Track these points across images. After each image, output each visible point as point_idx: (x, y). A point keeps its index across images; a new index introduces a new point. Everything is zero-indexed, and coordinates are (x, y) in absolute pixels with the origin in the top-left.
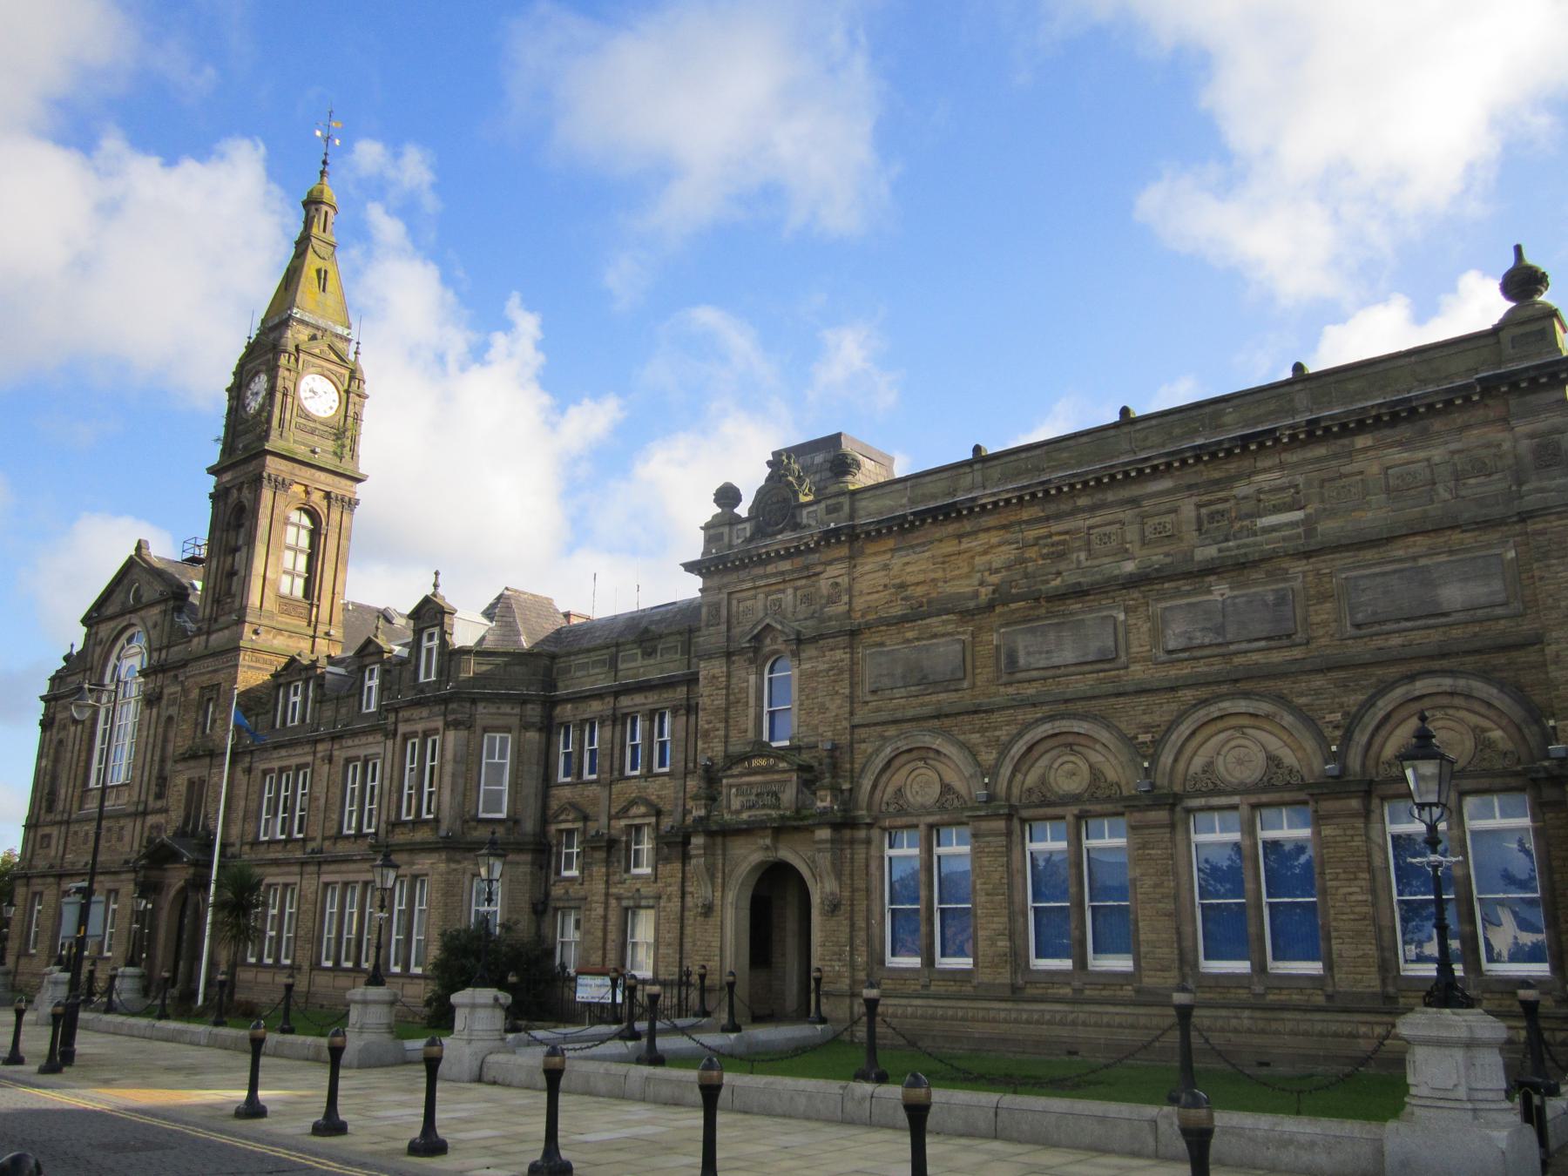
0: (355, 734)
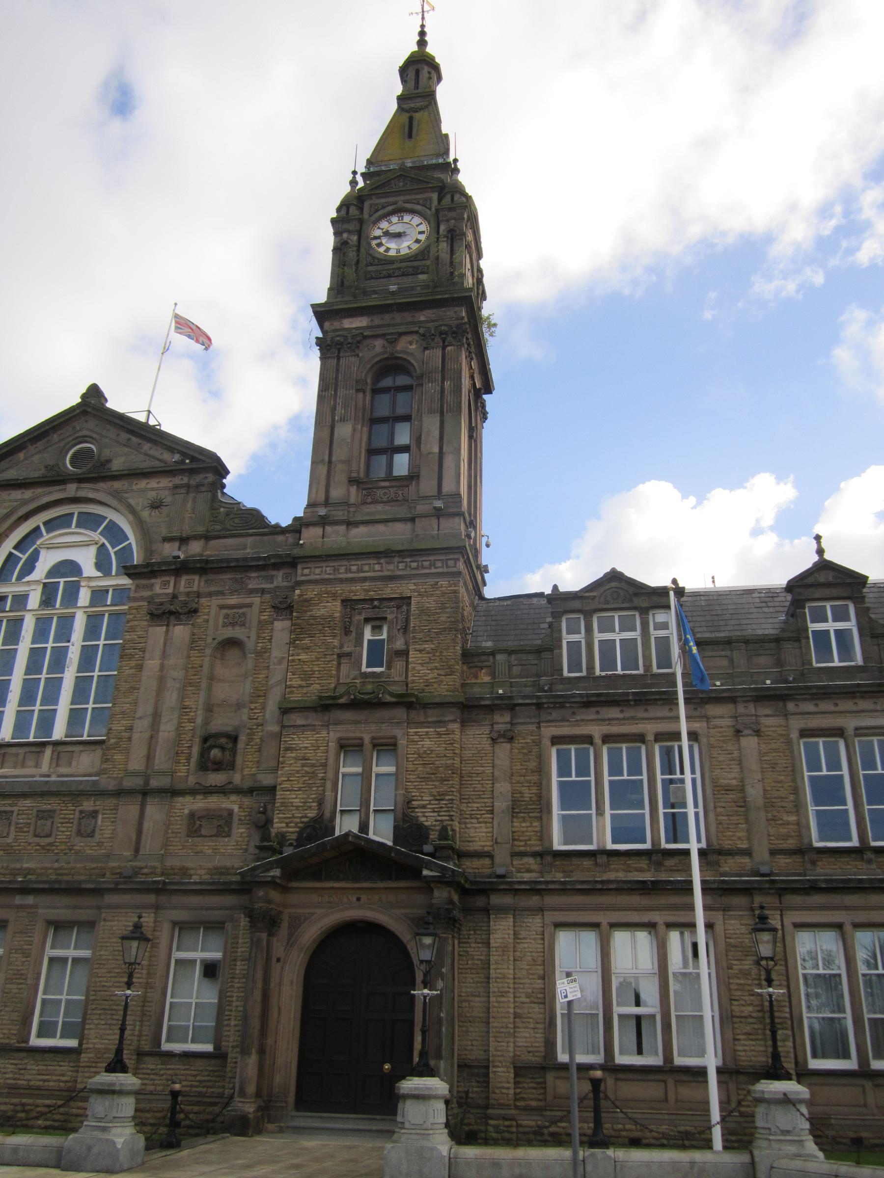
0: (825, 694)
